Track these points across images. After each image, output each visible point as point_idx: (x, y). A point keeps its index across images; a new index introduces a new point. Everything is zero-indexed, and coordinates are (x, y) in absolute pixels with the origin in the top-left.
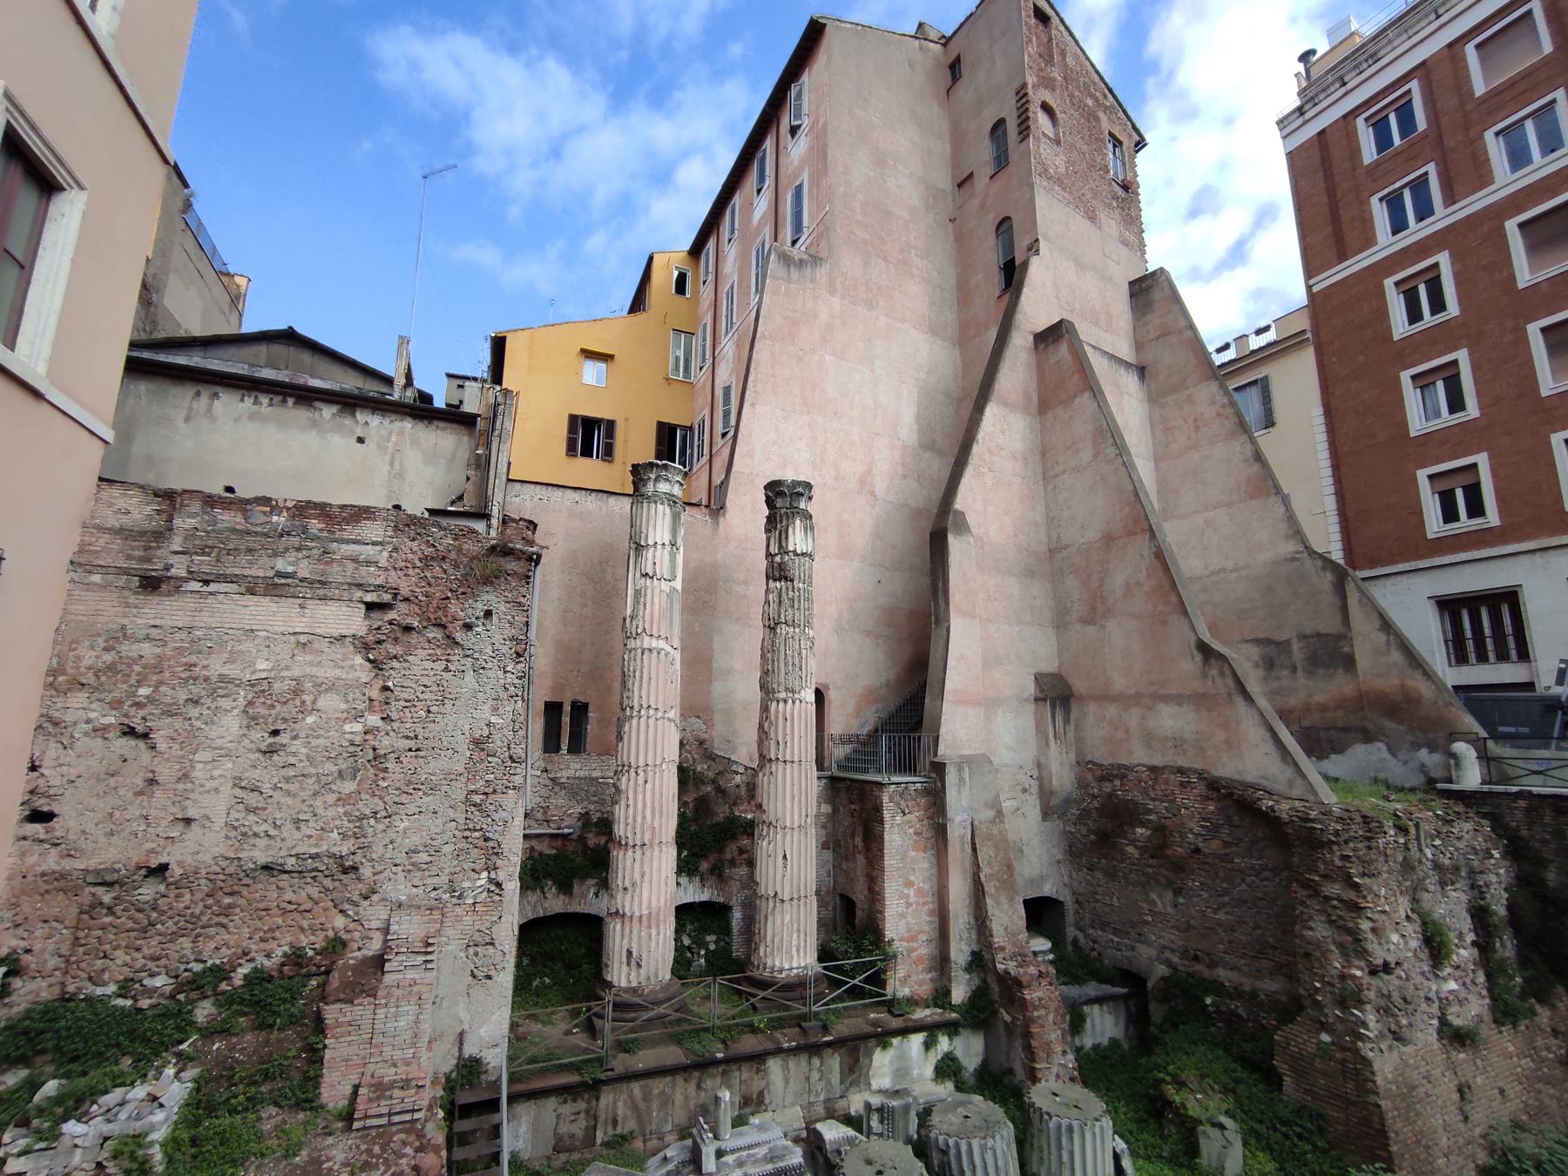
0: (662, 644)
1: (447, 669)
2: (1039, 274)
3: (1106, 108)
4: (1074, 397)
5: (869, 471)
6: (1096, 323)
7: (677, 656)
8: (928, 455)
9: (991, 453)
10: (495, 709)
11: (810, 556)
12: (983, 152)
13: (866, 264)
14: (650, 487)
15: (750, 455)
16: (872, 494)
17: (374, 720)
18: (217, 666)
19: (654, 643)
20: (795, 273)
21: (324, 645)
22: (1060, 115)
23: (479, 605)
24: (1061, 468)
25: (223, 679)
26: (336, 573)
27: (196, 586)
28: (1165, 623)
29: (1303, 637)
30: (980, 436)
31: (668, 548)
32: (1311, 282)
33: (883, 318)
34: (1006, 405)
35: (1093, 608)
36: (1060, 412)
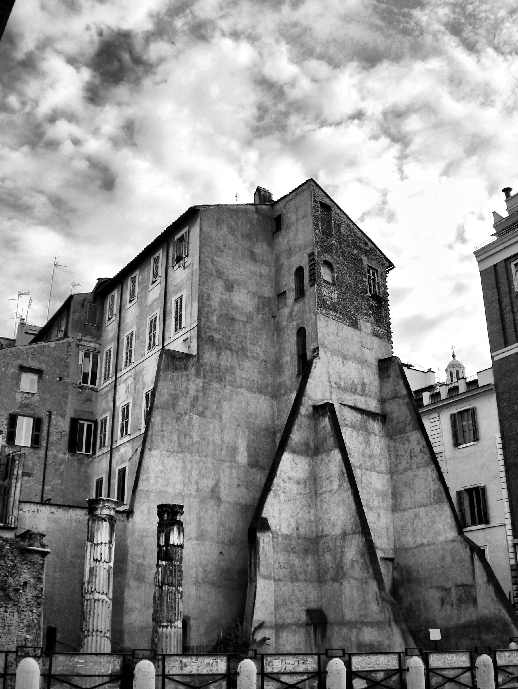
0: (104, 597)
1: (6, 611)
2: (318, 369)
3: (366, 251)
4: (332, 450)
5: (217, 485)
6: (355, 392)
7: (110, 602)
8: (254, 470)
10: (27, 632)
11: (181, 546)
12: (289, 282)
13: (219, 355)
14: (99, 512)
15: (148, 479)
16: (219, 499)
19: (100, 596)
22: (335, 266)
23: (21, 579)
24: (324, 490)
28: (367, 583)
29: (457, 586)
30: (278, 473)
31: (108, 545)
32: (493, 354)
33: (228, 387)
34: (294, 452)
35: (337, 573)
36: (324, 456)
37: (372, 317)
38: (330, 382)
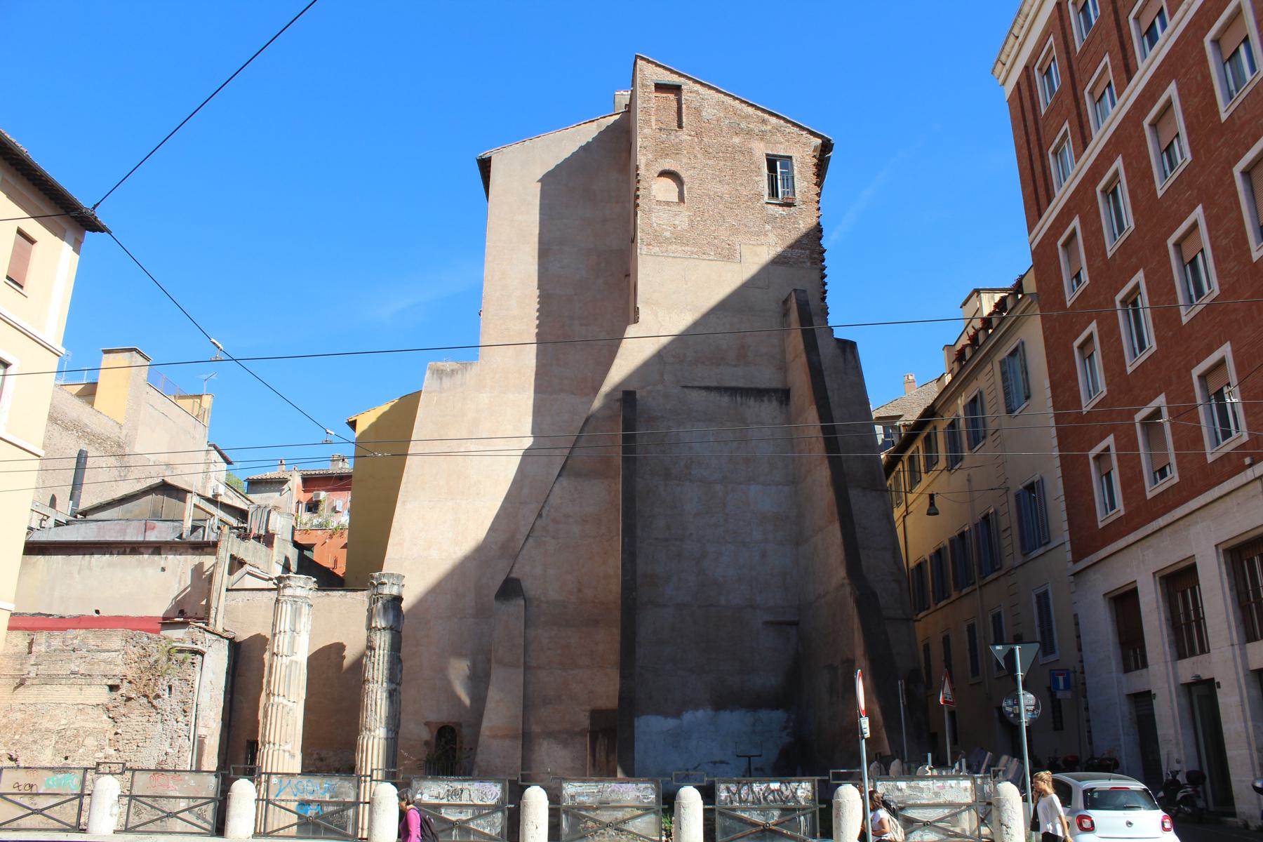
9: (555, 521)
17: (111, 751)
18: (46, 723)
20: (447, 382)
21: (89, 710)
25: (48, 730)
37: (770, 235)
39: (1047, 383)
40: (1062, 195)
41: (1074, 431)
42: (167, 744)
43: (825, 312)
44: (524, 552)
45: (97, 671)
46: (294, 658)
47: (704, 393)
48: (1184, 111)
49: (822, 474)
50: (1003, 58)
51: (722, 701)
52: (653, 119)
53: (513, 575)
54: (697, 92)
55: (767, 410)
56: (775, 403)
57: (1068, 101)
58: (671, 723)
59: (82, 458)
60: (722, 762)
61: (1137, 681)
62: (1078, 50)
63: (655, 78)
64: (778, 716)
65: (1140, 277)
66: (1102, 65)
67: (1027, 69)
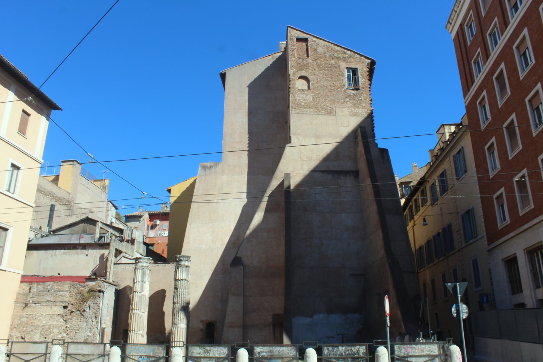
17: (65, 335)
18: (37, 323)
20: (208, 171)
21: (55, 317)
25: (37, 326)
26: (58, 300)
27: (34, 305)
37: (349, 103)
38: (301, 158)
39: (474, 165)
40: (478, 80)
41: (487, 186)
42: (88, 331)
43: (374, 136)
44: (243, 245)
45: (58, 300)
46: (143, 293)
47: (320, 174)
48: (531, 41)
49: (373, 208)
50: (451, 21)
51: (330, 310)
52: (296, 53)
53: (238, 255)
54: (315, 41)
55: (349, 181)
56: (352, 177)
57: (480, 39)
58: (308, 320)
59: (52, 208)
60: (331, 337)
61: (518, 298)
62: (483, 16)
63: (296, 35)
64: (356, 316)
65: (513, 116)
66: (494, 22)
67: (461, 26)
